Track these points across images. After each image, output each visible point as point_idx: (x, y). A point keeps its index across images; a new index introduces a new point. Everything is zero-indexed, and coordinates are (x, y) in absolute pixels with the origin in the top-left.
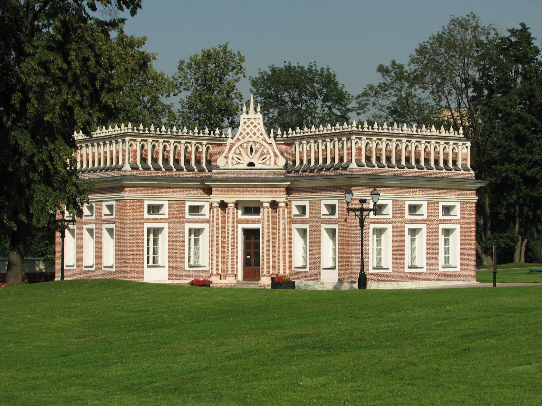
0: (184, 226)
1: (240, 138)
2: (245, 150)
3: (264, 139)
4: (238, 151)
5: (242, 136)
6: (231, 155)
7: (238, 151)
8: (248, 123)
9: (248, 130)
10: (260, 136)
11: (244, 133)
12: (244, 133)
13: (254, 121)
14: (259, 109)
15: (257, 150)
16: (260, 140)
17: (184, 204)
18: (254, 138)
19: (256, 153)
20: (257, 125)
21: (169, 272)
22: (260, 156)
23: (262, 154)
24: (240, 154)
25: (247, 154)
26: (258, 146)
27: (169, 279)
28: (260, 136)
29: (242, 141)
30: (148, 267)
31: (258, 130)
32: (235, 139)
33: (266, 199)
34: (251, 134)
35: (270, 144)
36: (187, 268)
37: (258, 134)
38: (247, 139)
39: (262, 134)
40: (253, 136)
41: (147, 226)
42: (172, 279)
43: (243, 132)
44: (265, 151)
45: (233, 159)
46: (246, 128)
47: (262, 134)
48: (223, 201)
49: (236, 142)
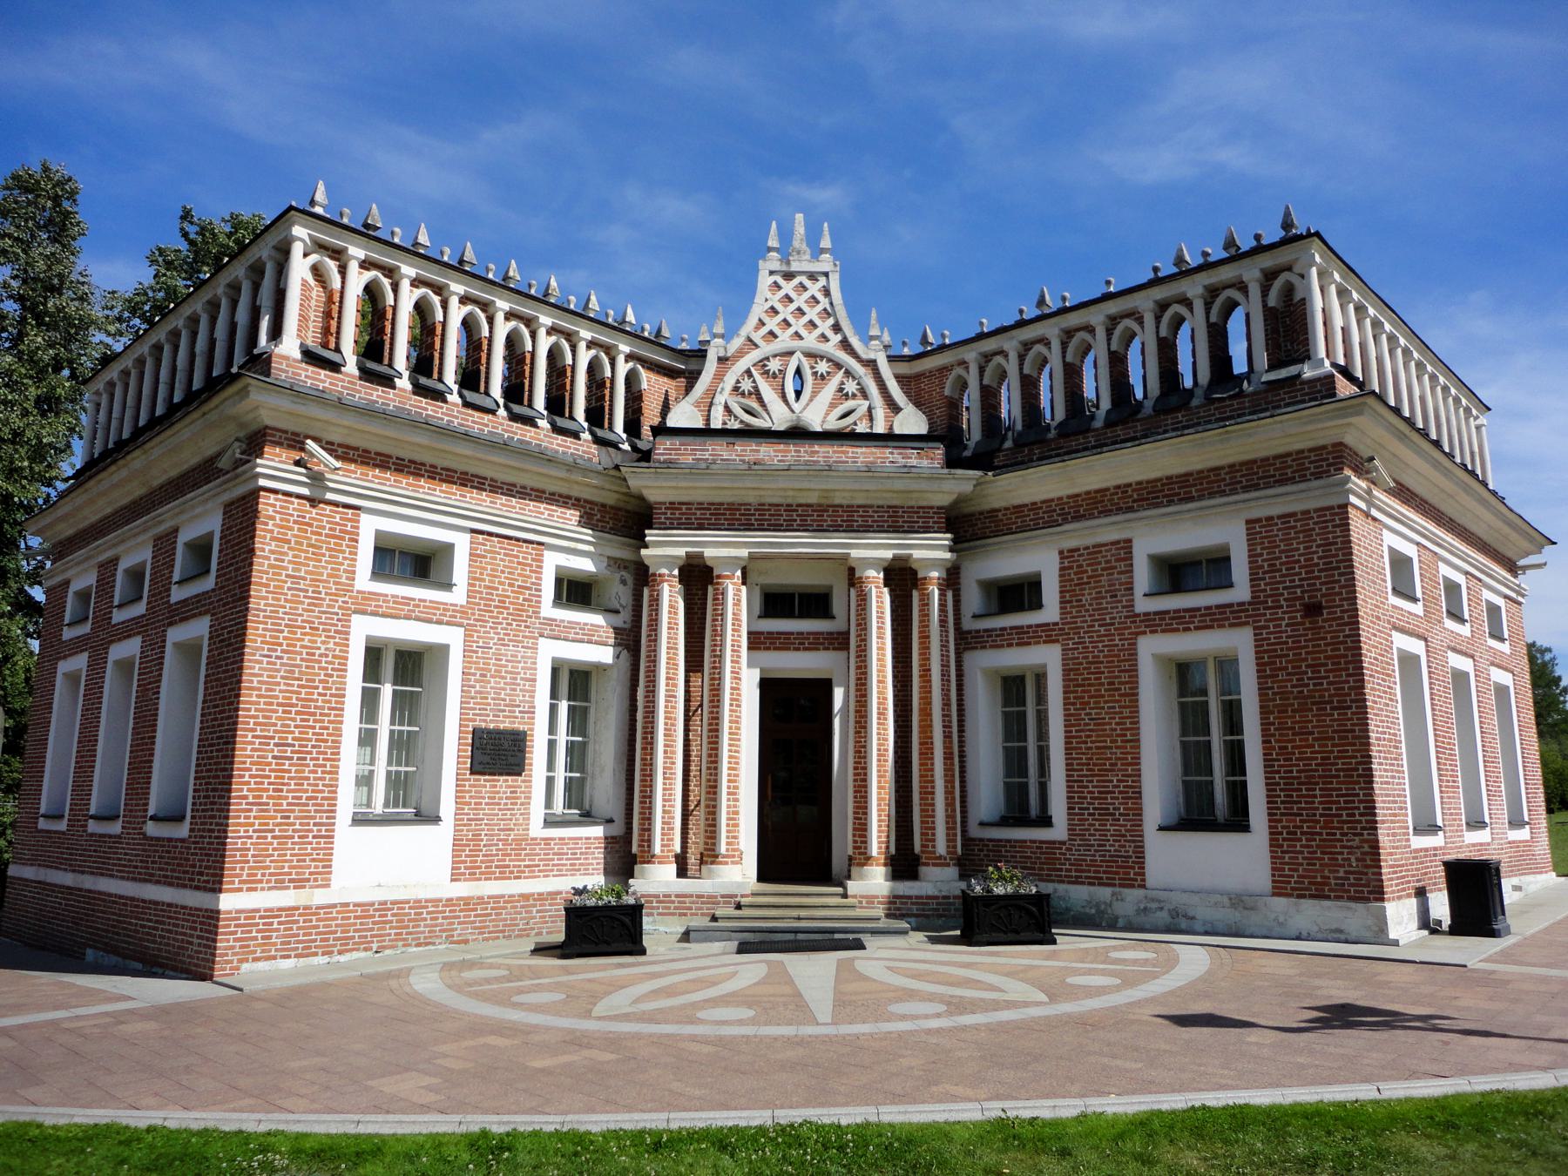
0: (535, 648)
1: (757, 337)
2: (776, 377)
3: (845, 345)
4: (746, 385)
5: (764, 330)
6: (720, 399)
7: (746, 385)
8: (788, 287)
9: (786, 312)
10: (830, 334)
11: (772, 324)
12: (772, 324)
13: (807, 283)
14: (826, 242)
15: (822, 378)
16: (832, 347)
17: (539, 560)
18: (810, 341)
19: (814, 394)
20: (820, 296)
21: (457, 845)
22: (833, 406)
23: (842, 394)
24: (757, 394)
25: (784, 397)
26: (823, 367)
27: (455, 878)
28: (830, 334)
29: (766, 349)
30: (359, 820)
31: (826, 313)
32: (737, 343)
33: (872, 551)
34: (798, 325)
35: (871, 364)
36: (536, 829)
37: (825, 326)
38: (784, 341)
39: (837, 328)
40: (803, 333)
41: (363, 629)
42: (473, 877)
43: (766, 319)
44: (851, 387)
45: (727, 408)
46: (779, 307)
47: (837, 328)
48: (700, 556)
49: (741, 353)
